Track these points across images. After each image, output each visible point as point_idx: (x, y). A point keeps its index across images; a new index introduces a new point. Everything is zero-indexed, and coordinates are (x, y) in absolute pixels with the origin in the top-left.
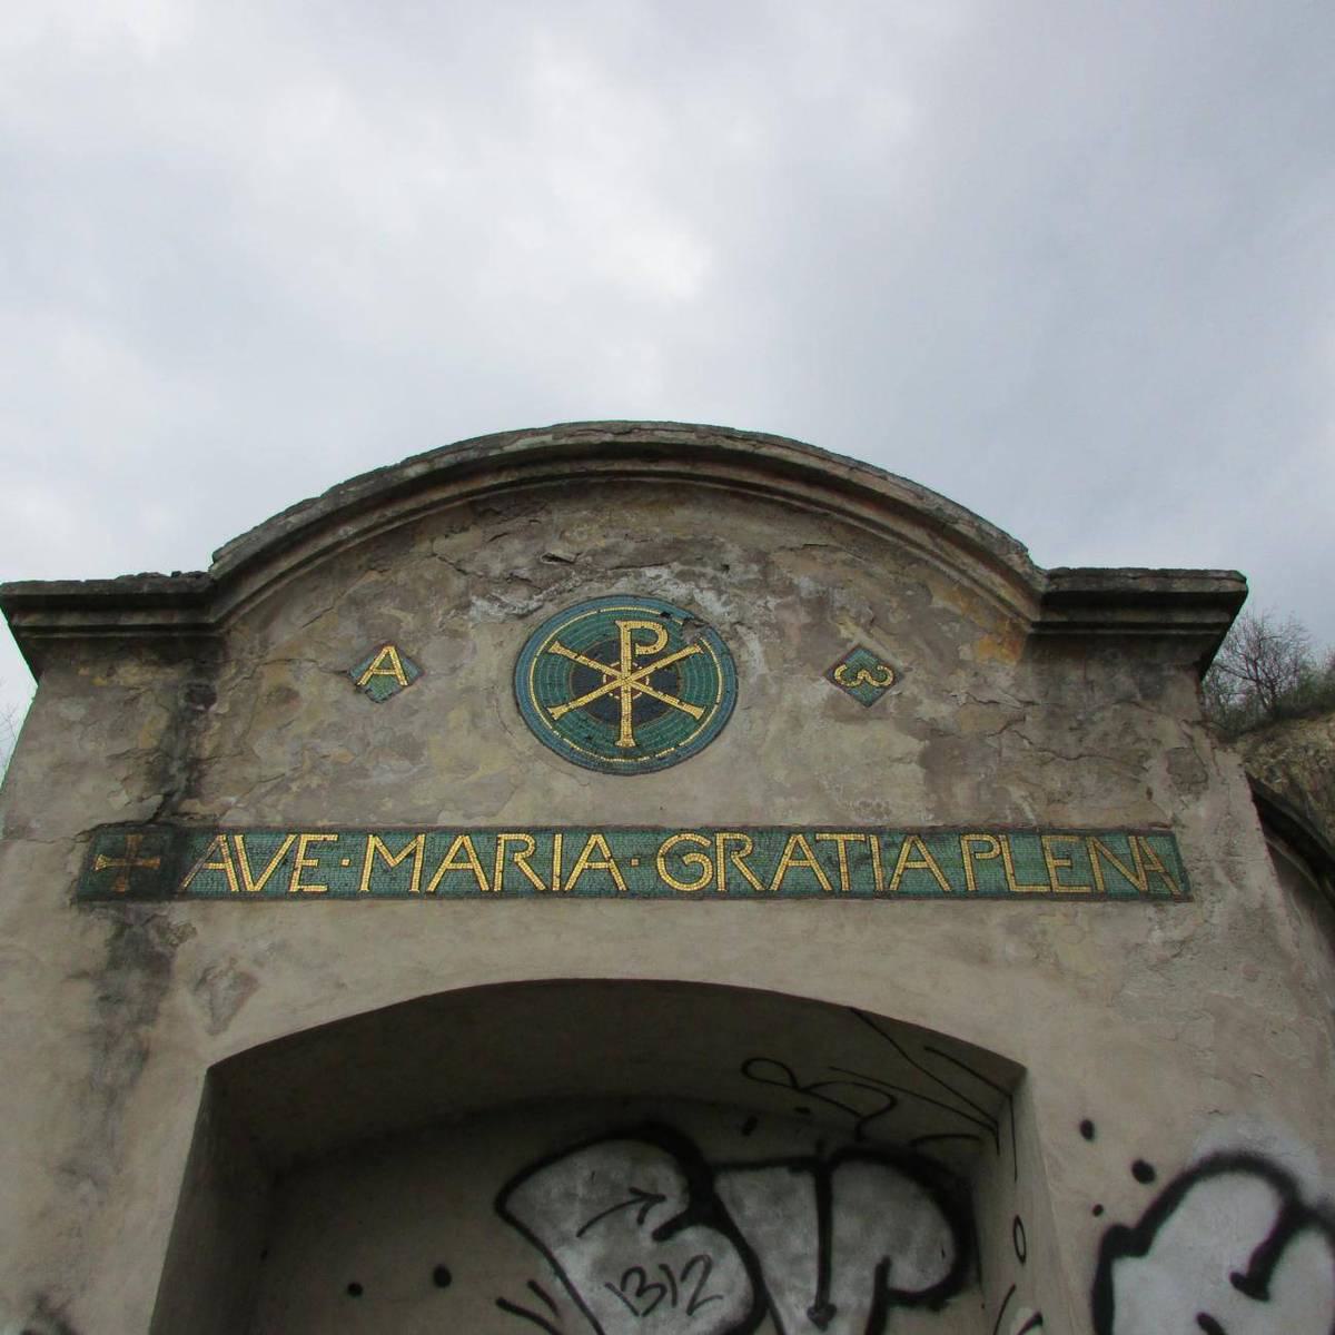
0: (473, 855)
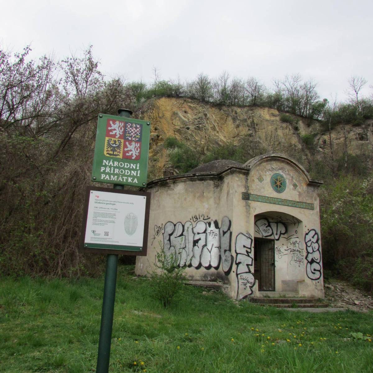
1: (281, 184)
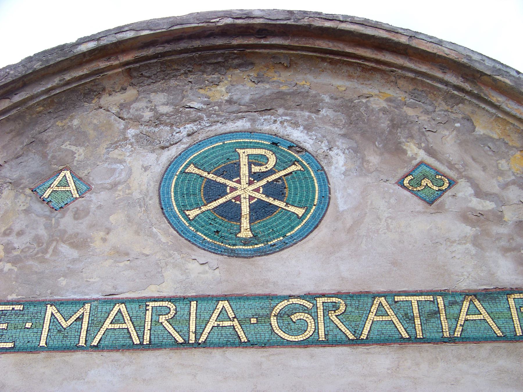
0: (127, 318)
1: (275, 190)
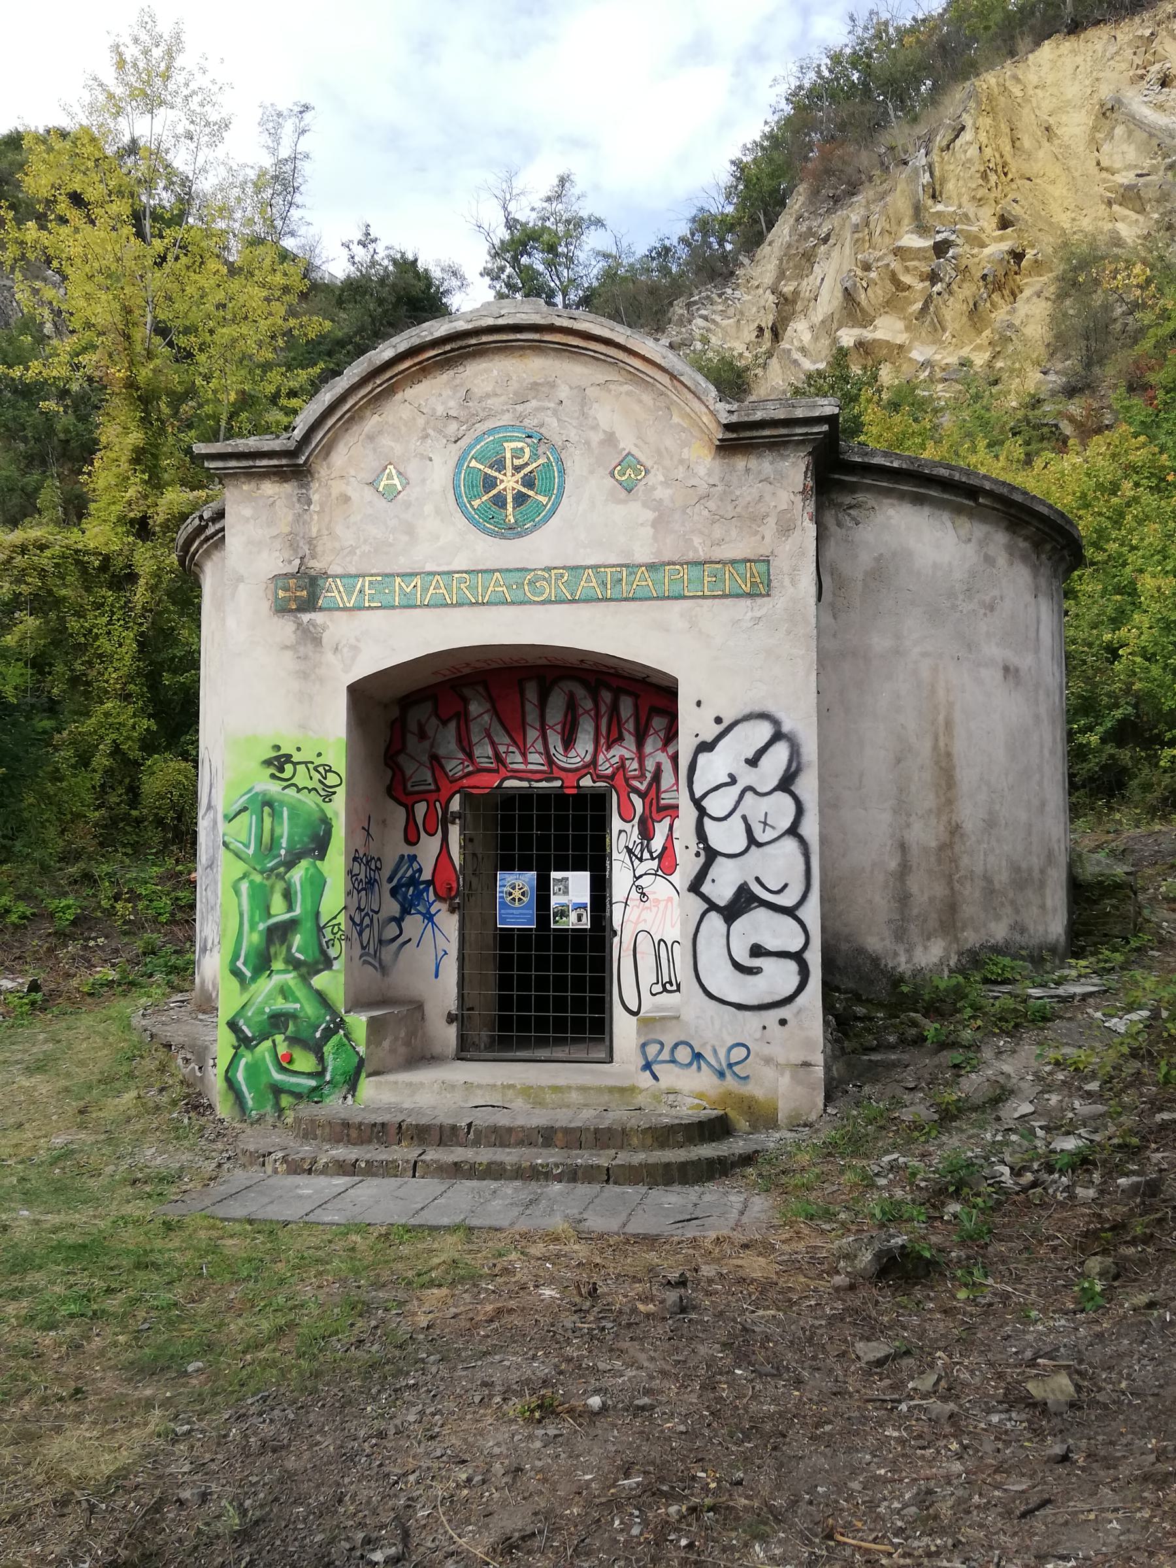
1: (529, 482)
